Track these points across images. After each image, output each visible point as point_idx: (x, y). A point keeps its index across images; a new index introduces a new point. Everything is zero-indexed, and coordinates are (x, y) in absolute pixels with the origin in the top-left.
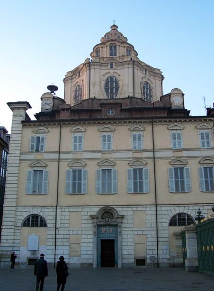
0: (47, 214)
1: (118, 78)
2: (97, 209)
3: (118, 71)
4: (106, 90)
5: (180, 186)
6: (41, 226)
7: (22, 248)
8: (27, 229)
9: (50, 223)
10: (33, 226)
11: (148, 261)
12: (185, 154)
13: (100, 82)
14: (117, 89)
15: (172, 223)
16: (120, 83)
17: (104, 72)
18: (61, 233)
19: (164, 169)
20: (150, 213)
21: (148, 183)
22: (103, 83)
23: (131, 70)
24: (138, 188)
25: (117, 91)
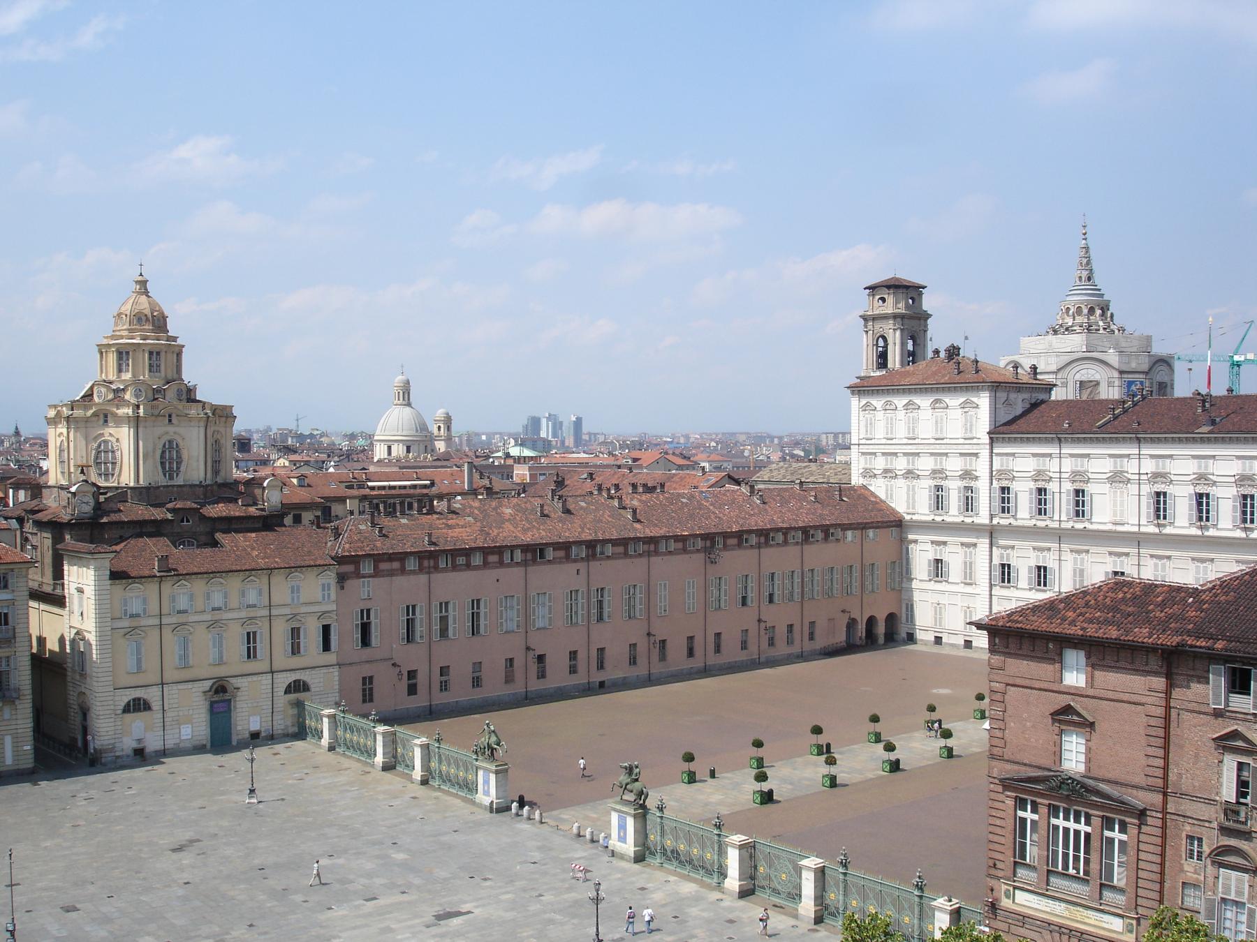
0: (152, 695)
1: (181, 444)
2: (209, 683)
3: (181, 430)
4: (163, 464)
5: (296, 650)
6: (145, 709)
7: (125, 739)
8: (129, 717)
9: (156, 705)
10: (135, 711)
11: (263, 734)
12: (304, 609)
13: (154, 452)
14: (179, 464)
15: (288, 690)
16: (185, 456)
17: (159, 430)
18: (169, 714)
19: (281, 630)
20: (265, 682)
21: (262, 647)
22: (159, 452)
23: (202, 430)
24: (251, 654)
25: (178, 468)
